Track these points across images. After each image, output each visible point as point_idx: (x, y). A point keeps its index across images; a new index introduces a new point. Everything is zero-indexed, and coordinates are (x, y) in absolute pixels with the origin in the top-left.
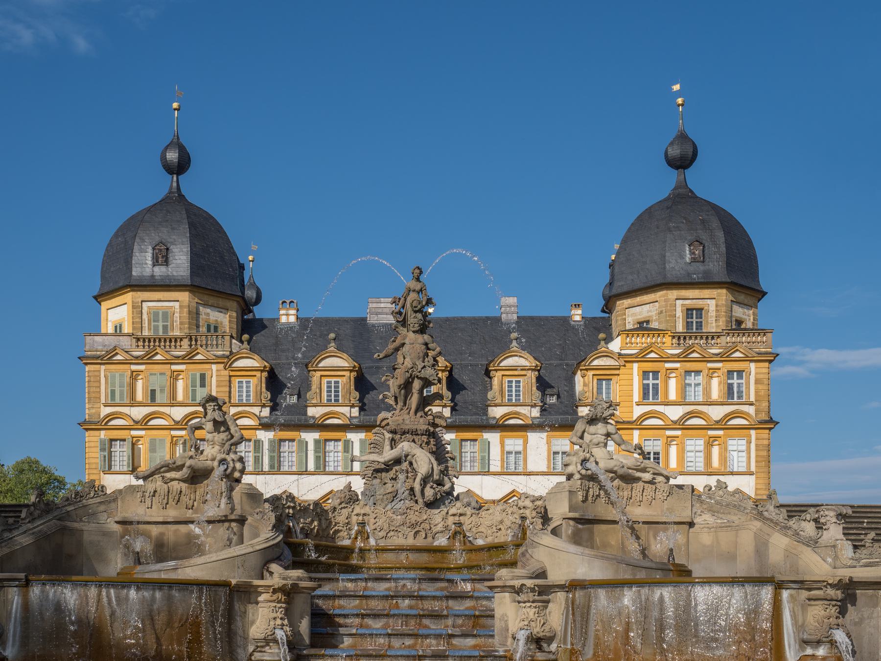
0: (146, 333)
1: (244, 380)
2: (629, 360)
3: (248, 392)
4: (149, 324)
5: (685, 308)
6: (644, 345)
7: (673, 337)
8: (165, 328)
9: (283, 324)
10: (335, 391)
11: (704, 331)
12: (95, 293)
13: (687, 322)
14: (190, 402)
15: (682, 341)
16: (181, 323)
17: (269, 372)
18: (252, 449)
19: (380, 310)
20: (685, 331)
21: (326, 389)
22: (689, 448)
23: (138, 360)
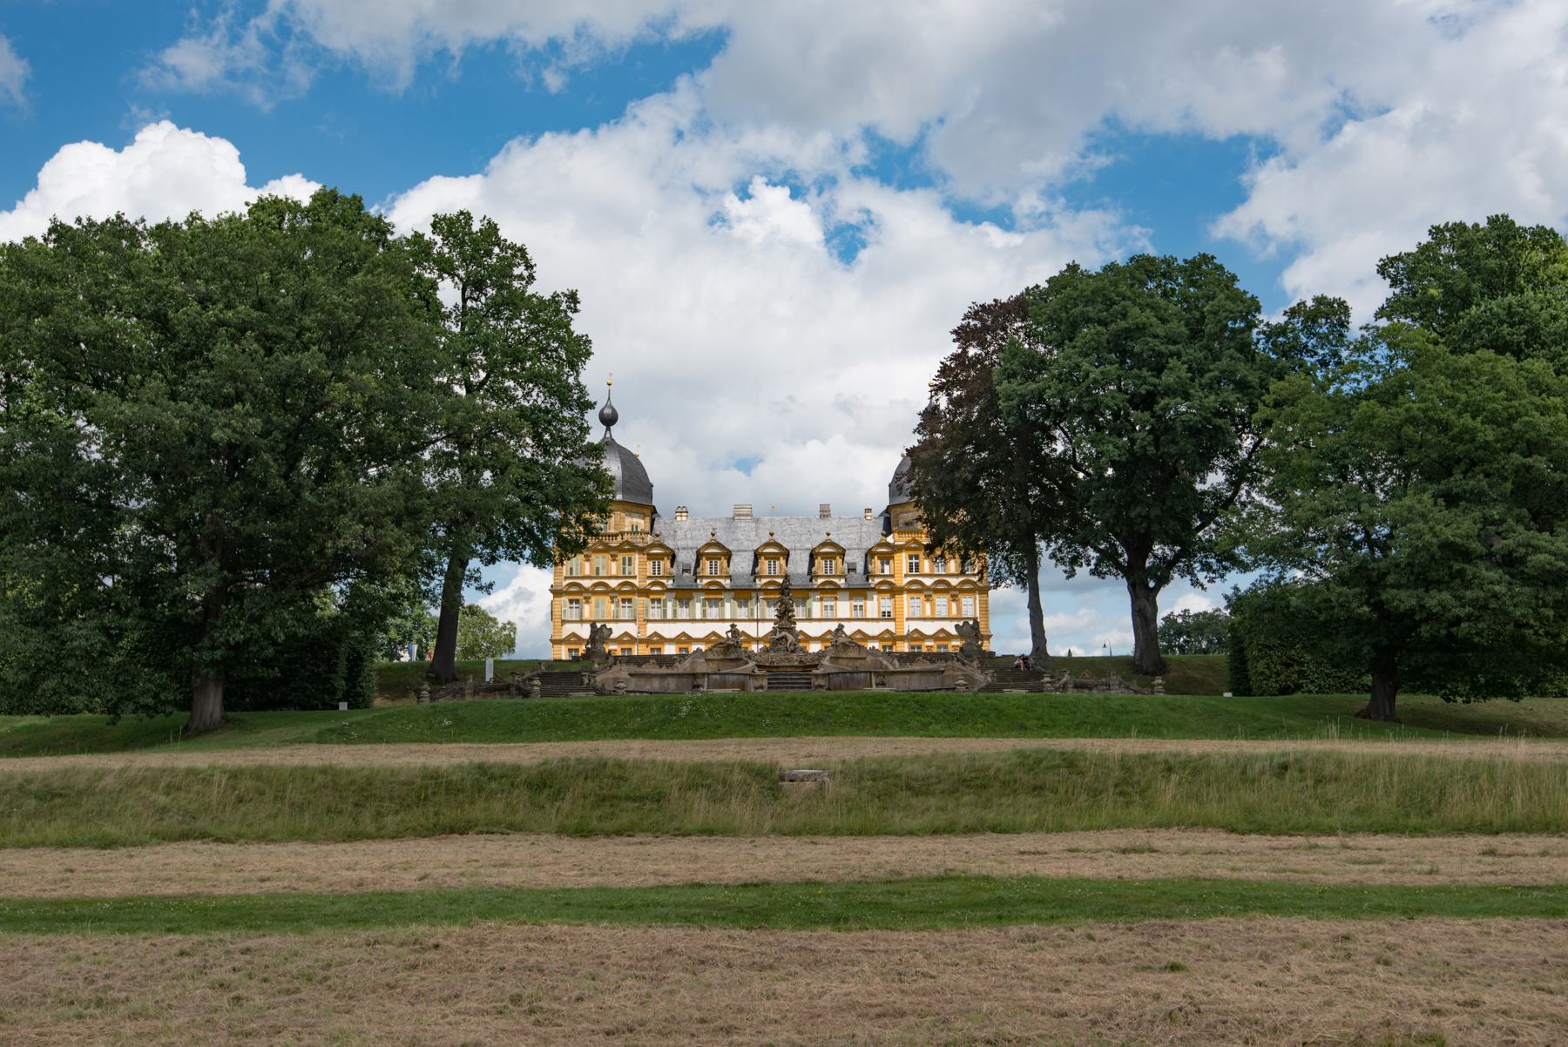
2: (899, 549)
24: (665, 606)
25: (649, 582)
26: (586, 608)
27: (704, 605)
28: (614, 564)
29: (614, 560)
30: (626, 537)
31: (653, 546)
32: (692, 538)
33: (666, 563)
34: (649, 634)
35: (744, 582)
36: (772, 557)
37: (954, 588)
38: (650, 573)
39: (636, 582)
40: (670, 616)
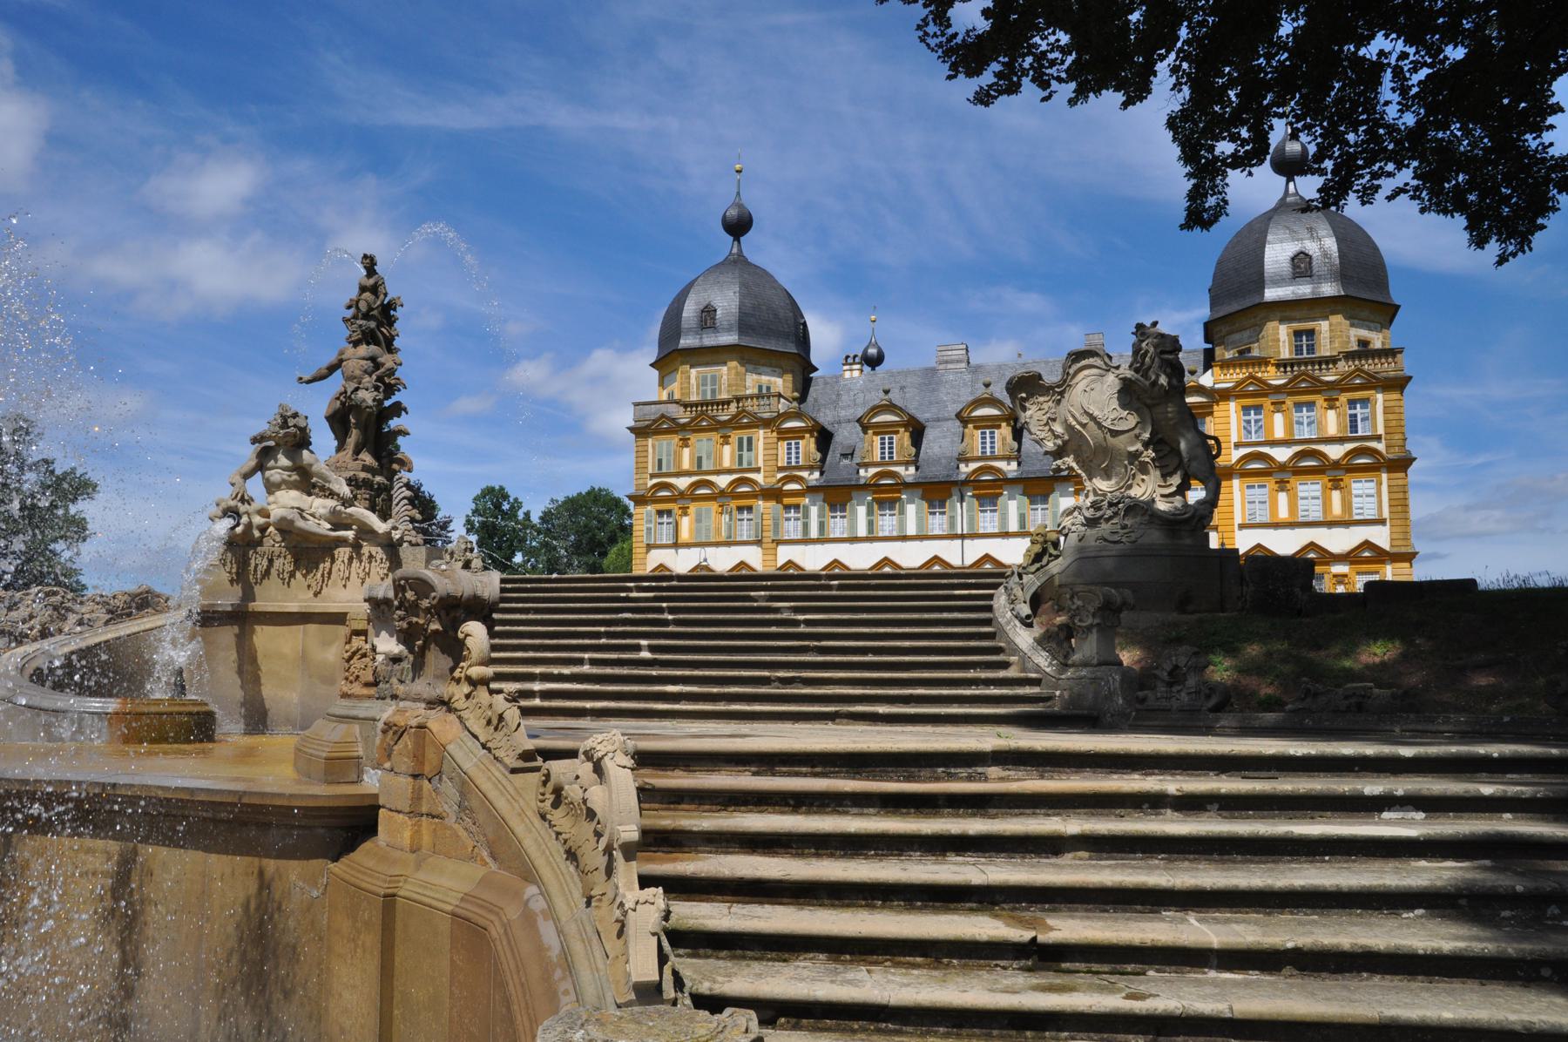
0: (694, 398)
1: (793, 442)
2: (1224, 395)
3: (797, 453)
4: (698, 388)
5: (1291, 331)
6: (1241, 376)
7: (1278, 366)
8: (713, 391)
9: (847, 379)
10: (889, 448)
11: (1317, 355)
12: (652, 361)
13: (1296, 346)
14: (736, 467)
15: (1289, 369)
16: (729, 386)
17: (818, 432)
18: (800, 515)
19: (949, 358)
20: (1294, 356)
21: (879, 446)
22: (1300, 494)
23: (683, 428)
24: (806, 515)
25: (780, 475)
26: (685, 522)
27: (870, 512)
28: (727, 449)
29: (727, 443)
30: (750, 406)
31: (787, 416)
32: (864, 403)
33: (808, 445)
34: (780, 563)
35: (936, 472)
36: (992, 422)
37: (1336, 465)
38: (782, 462)
39: (759, 478)
40: (814, 533)
